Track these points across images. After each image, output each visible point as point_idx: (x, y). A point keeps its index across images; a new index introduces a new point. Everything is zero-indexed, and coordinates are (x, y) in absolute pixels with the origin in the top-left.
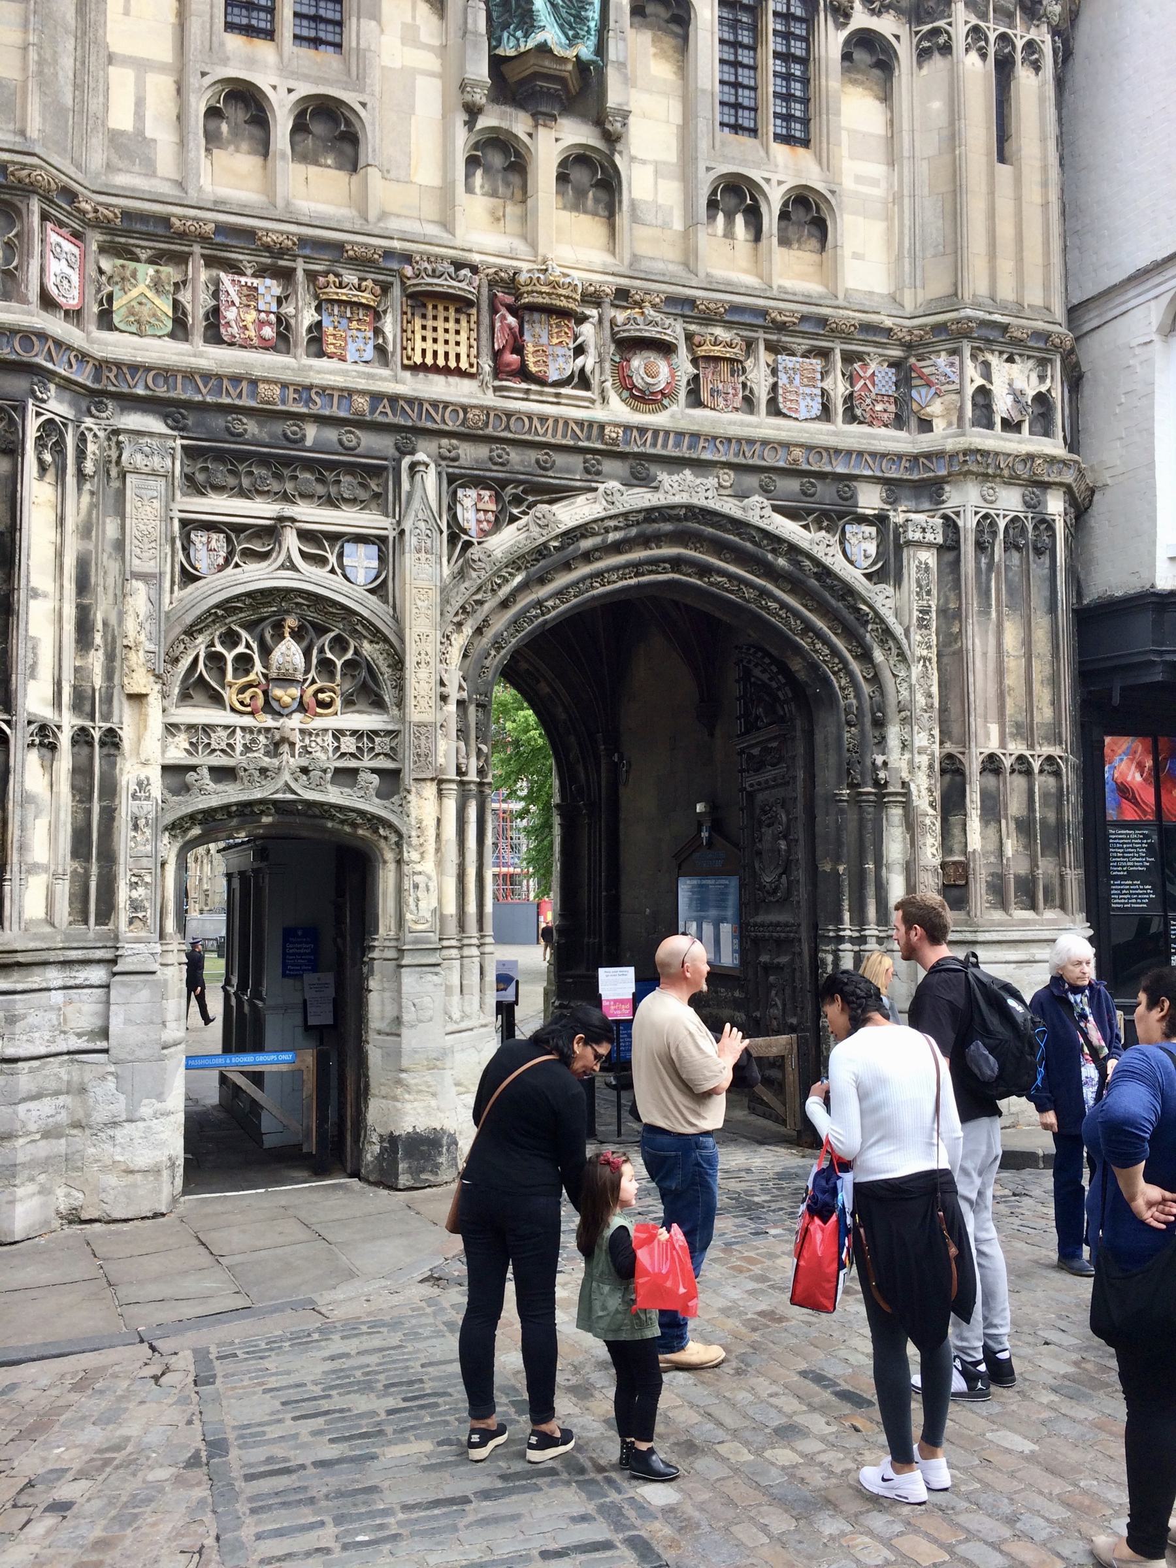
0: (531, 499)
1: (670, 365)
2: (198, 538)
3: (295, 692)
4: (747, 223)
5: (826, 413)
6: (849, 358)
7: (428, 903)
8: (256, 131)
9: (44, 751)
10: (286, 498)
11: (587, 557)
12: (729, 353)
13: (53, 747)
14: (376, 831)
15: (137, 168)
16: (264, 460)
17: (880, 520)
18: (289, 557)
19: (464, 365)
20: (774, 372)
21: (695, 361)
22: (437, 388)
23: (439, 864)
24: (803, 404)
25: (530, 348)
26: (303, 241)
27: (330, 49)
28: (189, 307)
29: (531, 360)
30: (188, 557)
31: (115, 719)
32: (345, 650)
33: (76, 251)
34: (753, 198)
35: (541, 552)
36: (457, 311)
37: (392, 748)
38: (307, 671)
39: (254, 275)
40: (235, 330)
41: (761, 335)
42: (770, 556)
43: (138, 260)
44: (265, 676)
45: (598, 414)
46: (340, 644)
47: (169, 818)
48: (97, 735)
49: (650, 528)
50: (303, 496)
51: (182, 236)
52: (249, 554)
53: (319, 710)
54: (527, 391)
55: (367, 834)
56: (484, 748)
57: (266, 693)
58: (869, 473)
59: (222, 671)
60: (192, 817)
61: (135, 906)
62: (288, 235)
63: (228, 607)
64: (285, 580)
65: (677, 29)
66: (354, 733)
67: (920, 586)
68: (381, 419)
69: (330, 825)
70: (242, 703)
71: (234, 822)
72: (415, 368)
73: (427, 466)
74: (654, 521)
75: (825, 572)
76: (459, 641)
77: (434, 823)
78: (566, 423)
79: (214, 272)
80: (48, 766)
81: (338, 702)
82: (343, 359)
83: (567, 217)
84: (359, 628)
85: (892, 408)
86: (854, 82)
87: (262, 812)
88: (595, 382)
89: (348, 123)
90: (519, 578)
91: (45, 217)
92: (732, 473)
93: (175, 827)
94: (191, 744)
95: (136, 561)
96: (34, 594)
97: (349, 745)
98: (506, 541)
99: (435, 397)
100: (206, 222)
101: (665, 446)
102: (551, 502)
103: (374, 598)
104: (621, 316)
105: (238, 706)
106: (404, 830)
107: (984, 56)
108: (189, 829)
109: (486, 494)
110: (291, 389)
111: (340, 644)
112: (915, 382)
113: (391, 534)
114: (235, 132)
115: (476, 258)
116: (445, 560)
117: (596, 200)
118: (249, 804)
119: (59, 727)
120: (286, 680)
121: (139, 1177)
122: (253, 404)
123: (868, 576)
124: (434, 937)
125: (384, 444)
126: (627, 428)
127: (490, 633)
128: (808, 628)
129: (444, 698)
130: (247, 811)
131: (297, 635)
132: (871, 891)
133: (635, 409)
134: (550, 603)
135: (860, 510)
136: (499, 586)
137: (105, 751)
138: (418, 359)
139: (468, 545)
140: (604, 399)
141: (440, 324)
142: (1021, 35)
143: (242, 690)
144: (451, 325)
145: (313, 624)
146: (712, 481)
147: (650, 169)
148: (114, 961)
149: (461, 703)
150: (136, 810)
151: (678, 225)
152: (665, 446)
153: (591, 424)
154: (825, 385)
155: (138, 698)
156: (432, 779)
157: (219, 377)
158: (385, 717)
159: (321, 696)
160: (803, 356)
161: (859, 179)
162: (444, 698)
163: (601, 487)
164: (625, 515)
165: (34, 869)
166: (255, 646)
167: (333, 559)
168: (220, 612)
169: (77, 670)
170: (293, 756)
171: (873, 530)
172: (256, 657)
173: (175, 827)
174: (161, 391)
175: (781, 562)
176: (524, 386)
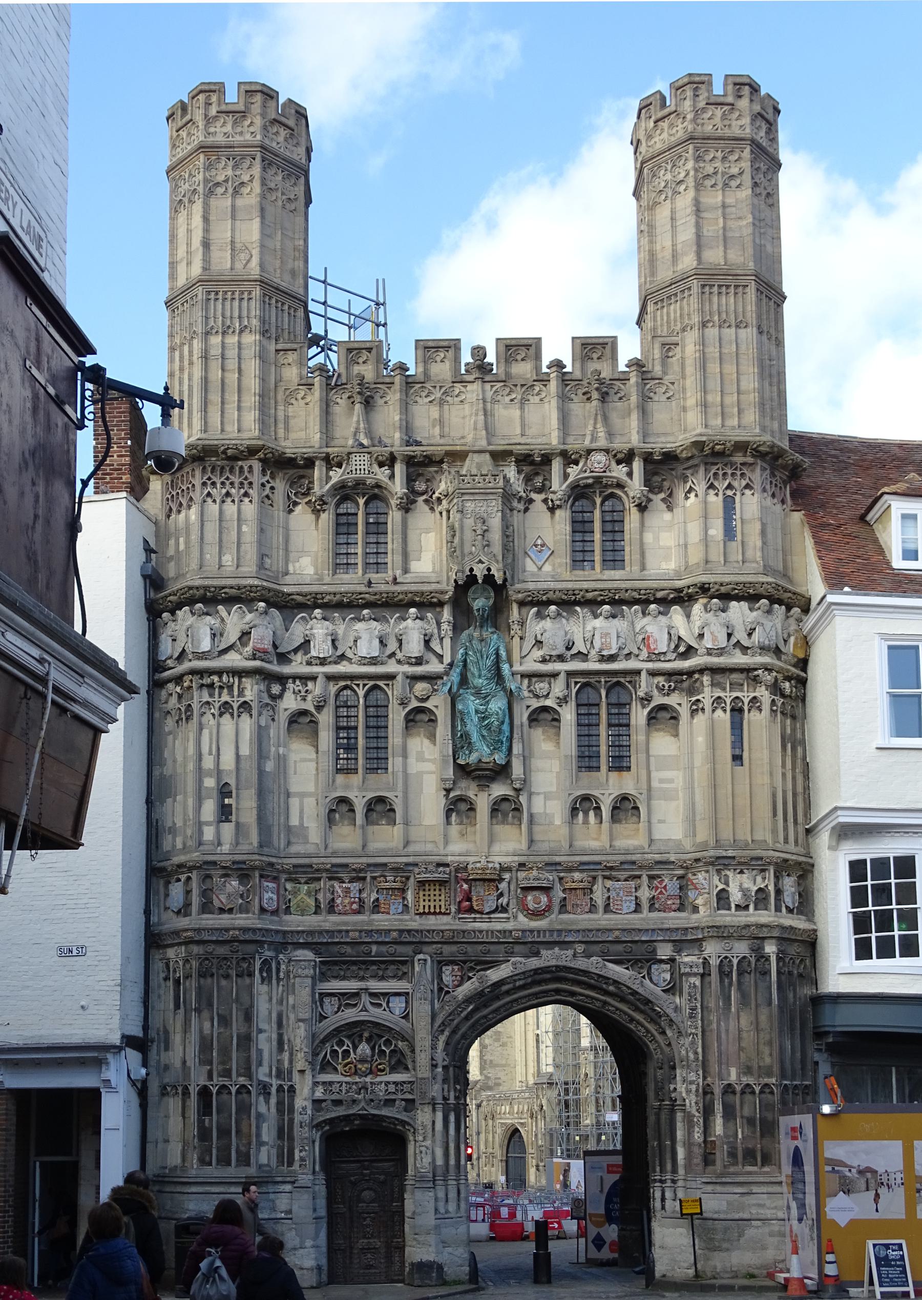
0: (478, 968)
1: (548, 896)
2: (326, 1000)
3: (366, 1065)
4: (596, 815)
5: (638, 909)
6: (651, 878)
7: (427, 1160)
8: (350, 814)
10: (362, 979)
11: (508, 993)
12: (582, 885)
13: (269, 1094)
15: (301, 841)
16: (354, 963)
17: (672, 960)
18: (364, 1006)
19: (443, 910)
20: (609, 890)
21: (564, 891)
22: (432, 922)
23: (434, 1141)
24: (625, 905)
25: (474, 898)
26: (369, 865)
27: (383, 771)
28: (322, 900)
29: (475, 904)
33: (274, 885)
34: (597, 803)
35: (481, 994)
36: (440, 885)
38: (373, 1056)
39: (349, 882)
40: (340, 908)
41: (600, 873)
42: (604, 986)
43: (300, 883)
45: (509, 926)
46: (388, 1043)
47: (315, 1122)
48: (286, 1088)
49: (538, 977)
50: (371, 977)
51: (318, 870)
52: (348, 1005)
54: (475, 918)
56: (458, 1087)
57: (355, 1066)
58: (662, 938)
60: (324, 1121)
61: (302, 1159)
62: (362, 864)
63: (338, 1030)
64: (363, 1016)
65: (555, 723)
66: (394, 1083)
67: (690, 995)
68: (405, 940)
69: (384, 1124)
71: (343, 1124)
72: (420, 914)
73: (425, 960)
74: (540, 974)
75: (635, 993)
76: (443, 1039)
77: (431, 1124)
78: (492, 932)
79: (332, 882)
80: (267, 1102)
81: (388, 1069)
82: (388, 913)
83: (498, 828)
85: (678, 901)
86: (657, 730)
88: (510, 909)
89: (391, 804)
90: (471, 1007)
91: (261, 876)
92: (583, 946)
93: (318, 1126)
96: (260, 1031)
97: (392, 1088)
98: (467, 988)
99: (428, 928)
100: (327, 864)
101: (544, 936)
102: (485, 970)
103: (404, 1021)
104: (522, 875)
106: (416, 1126)
107: (725, 711)
109: (456, 968)
111: (388, 1043)
112: (690, 887)
113: (411, 991)
114: (341, 817)
115: (450, 859)
116: (436, 1001)
117: (513, 817)
120: (363, 1061)
121: (305, 1271)
122: (348, 940)
123: (663, 991)
124: (431, 1175)
125: (409, 950)
126: (523, 931)
127: (460, 1033)
128: (632, 1020)
129: (434, 1066)
131: (368, 1041)
132: (668, 1156)
133: (531, 919)
134: (490, 1016)
135: (658, 957)
136: (461, 1012)
138: (421, 910)
139: (448, 992)
140: (515, 917)
141: (432, 893)
142: (746, 696)
143: (345, 1065)
144: (437, 892)
146: (570, 952)
147: (542, 796)
148: (293, 1182)
149: (444, 1067)
151: (558, 822)
152: (544, 936)
153: (505, 931)
154: (637, 894)
155: (302, 1072)
157: (333, 932)
160: (626, 880)
161: (661, 781)
162: (434, 1066)
163: (513, 959)
164: (523, 973)
165: (261, 1144)
167: (384, 1005)
169: (278, 1061)
171: (668, 966)
173: (318, 1126)
174: (310, 940)
175: (611, 988)
176: (473, 916)
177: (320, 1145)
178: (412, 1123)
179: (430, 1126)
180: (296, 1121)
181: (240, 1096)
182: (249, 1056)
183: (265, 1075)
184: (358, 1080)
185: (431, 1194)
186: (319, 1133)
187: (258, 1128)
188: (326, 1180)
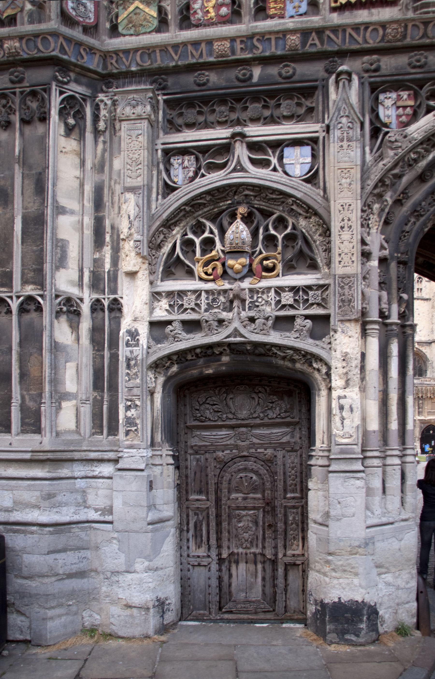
3: (244, 260)
9: (71, 316)
10: (238, 122)
13: (78, 314)
14: (311, 365)
18: (239, 162)
30: (169, 175)
31: (119, 292)
32: (286, 227)
37: (323, 299)
38: (254, 245)
44: (223, 251)
47: (153, 358)
48: (106, 303)
53: (264, 274)
55: (305, 368)
57: (223, 265)
59: (194, 252)
70: (206, 273)
71: (201, 361)
77: (359, 356)
81: (280, 267)
84: (294, 207)
87: (221, 353)
94: (170, 305)
95: (129, 180)
105: (204, 276)
106: (334, 364)
108: (169, 368)
110: (238, 41)
118: (210, 346)
119: (81, 300)
122: (212, 59)
124: (358, 449)
130: (209, 352)
137: (113, 315)
143: (206, 264)
145: (261, 211)
150: (129, 355)
155: (132, 275)
156: (356, 320)
158: (318, 276)
159: (265, 262)
166: (216, 231)
167: (274, 161)
168: (188, 208)
170: (244, 310)
172: (217, 239)
177: (163, 399)
178: (323, 354)
179: (356, 362)
180: (120, 358)
181: (27, 317)
182: (42, 250)
183: (71, 283)
184: (227, 286)
185: (359, 483)
186: (161, 380)
187: (55, 367)
188: (173, 456)
